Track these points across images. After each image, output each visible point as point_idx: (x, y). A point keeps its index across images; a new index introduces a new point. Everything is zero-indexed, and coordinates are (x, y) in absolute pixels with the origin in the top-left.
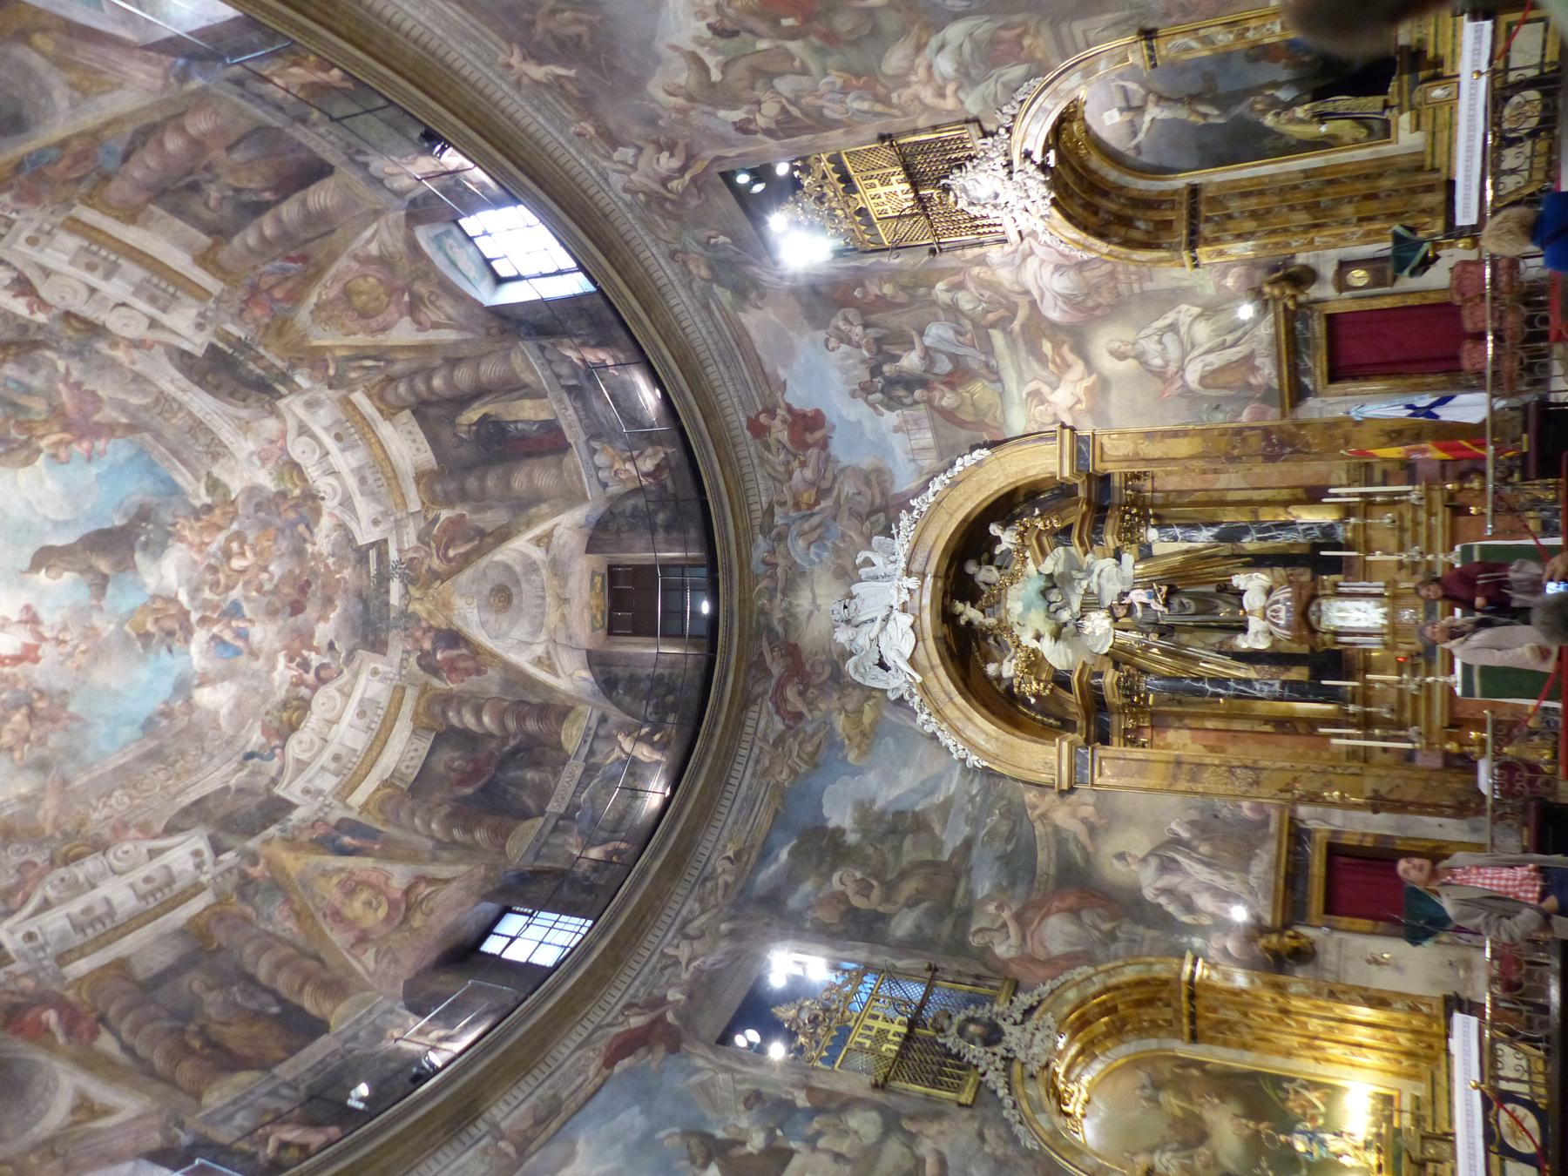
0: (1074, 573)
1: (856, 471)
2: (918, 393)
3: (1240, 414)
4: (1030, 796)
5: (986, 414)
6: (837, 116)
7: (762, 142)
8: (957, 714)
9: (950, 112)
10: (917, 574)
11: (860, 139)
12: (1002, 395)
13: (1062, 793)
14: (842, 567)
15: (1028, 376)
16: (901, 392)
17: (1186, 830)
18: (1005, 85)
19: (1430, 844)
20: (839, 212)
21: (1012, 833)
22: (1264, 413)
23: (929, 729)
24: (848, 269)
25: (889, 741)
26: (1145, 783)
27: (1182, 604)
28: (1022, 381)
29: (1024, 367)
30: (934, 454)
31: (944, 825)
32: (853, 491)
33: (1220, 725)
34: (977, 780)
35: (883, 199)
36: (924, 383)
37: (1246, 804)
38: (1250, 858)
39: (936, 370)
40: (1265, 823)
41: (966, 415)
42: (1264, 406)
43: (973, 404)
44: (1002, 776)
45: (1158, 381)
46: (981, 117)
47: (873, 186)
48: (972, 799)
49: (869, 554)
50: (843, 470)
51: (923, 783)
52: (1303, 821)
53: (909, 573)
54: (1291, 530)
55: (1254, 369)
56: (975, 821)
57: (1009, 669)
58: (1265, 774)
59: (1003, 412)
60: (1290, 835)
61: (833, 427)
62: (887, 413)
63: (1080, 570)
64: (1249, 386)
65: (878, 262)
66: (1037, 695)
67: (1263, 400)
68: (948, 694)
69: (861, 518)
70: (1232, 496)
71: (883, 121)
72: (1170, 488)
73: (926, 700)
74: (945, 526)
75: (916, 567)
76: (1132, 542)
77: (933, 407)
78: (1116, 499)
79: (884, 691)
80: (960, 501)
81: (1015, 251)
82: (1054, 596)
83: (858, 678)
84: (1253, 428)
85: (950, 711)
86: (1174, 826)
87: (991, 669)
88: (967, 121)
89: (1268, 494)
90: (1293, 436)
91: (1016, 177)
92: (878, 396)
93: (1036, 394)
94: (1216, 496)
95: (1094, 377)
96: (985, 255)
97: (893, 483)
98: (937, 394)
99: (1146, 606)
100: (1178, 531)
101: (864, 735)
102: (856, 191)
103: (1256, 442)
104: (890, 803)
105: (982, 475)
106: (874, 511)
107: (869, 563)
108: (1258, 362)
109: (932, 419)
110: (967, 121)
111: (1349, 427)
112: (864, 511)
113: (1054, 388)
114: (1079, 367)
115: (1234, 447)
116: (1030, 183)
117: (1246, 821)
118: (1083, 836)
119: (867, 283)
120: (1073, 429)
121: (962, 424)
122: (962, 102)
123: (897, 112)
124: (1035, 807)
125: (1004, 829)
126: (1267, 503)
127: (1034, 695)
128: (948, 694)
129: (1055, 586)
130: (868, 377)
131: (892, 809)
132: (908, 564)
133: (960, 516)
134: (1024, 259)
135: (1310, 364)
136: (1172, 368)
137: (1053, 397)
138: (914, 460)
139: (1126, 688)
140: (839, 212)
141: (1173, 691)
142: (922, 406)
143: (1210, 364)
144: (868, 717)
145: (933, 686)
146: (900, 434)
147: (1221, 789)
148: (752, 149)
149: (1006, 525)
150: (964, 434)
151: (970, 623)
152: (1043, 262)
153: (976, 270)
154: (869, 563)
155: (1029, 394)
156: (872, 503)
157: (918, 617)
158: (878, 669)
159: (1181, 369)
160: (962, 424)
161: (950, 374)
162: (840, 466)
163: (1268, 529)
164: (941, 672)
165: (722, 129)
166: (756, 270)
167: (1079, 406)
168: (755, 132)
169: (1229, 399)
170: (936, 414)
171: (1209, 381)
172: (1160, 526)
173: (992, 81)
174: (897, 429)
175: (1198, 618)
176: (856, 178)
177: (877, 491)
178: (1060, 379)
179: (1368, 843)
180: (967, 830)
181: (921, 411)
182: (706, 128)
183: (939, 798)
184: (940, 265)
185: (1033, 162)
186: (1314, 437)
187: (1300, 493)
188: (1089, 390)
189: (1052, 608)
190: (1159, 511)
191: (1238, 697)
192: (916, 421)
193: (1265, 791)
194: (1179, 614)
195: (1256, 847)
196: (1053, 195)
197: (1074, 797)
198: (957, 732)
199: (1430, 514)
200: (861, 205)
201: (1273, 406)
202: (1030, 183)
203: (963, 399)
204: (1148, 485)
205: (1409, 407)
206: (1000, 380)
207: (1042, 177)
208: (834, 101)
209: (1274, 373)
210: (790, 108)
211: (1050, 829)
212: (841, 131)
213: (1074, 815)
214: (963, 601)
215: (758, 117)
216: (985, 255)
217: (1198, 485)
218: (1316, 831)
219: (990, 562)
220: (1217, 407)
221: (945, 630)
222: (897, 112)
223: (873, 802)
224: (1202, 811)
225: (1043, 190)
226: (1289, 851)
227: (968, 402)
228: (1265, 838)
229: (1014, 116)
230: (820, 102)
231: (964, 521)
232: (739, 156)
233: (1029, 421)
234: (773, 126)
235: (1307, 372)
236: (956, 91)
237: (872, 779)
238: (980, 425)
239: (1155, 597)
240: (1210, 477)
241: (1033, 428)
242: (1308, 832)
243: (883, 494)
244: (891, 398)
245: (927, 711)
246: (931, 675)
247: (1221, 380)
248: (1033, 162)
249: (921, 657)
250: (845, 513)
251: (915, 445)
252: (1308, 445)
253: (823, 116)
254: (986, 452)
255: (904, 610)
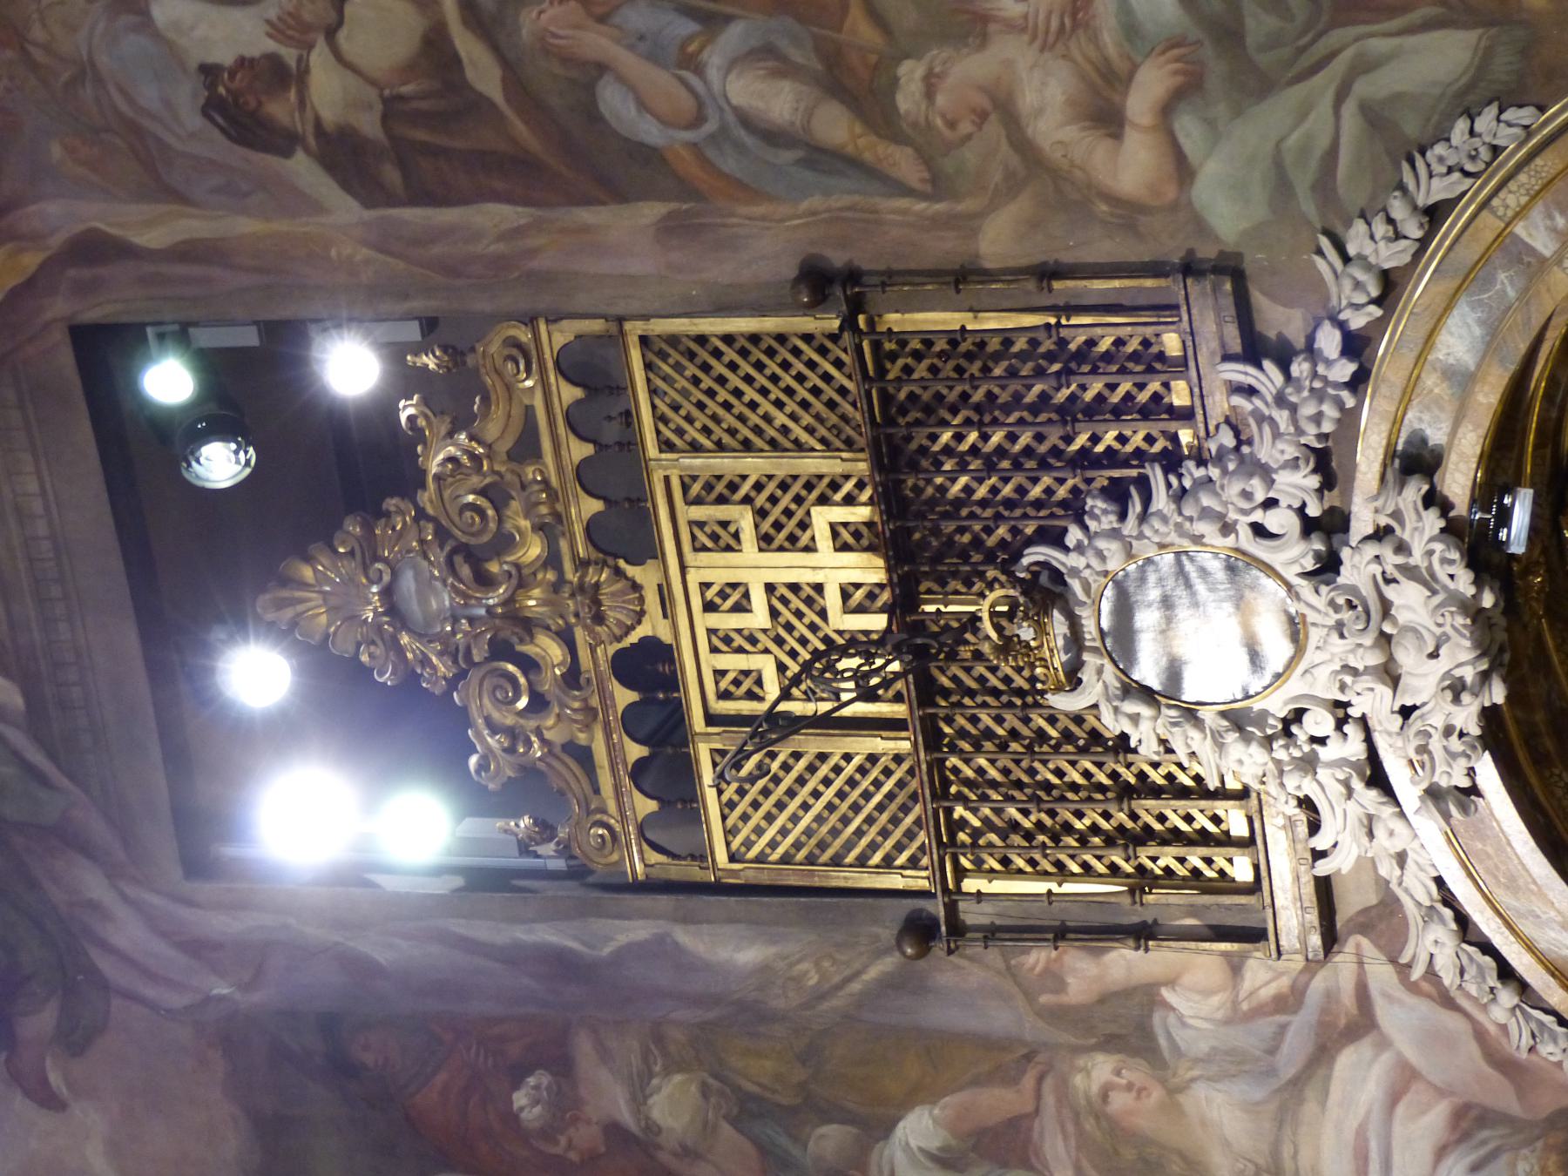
6: (650, 132)
7: (298, 202)
9: (1129, 213)
11: (722, 271)
18: (1376, 118)
20: (550, 650)
24: (514, 957)
35: (759, 618)
46: (1254, 260)
47: (724, 540)
65: (660, 949)
71: (841, 196)
81: (1288, 1002)
88: (1190, 268)
91: (1358, 568)
96: (1146, 997)
102: (648, 550)
110: (1190, 268)
116: (1409, 601)
119: (583, 1047)
122: (1183, 170)
123: (904, 163)
134: (1323, 1053)
140: (550, 650)
148: (245, 226)
152: (1404, 1080)
153: (1100, 1070)
165: (149, 95)
166: (93, 884)
168: (282, 142)
173: (1327, 82)
176: (664, 468)
182: (86, 71)
184: (941, 1016)
185: (1433, 499)
196: (1498, 694)
200: (653, 626)
202: (1409, 601)
207: (1464, 583)
208: (649, 47)
210: (467, 45)
212: (651, 211)
215: (319, 58)
216: (1146, 997)
222: (904, 163)
225: (1462, 657)
229: (1390, 286)
230: (596, 43)
232: (186, 252)
234: (369, 125)
236: (1167, 111)
248: (1433, 499)
253: (592, 115)
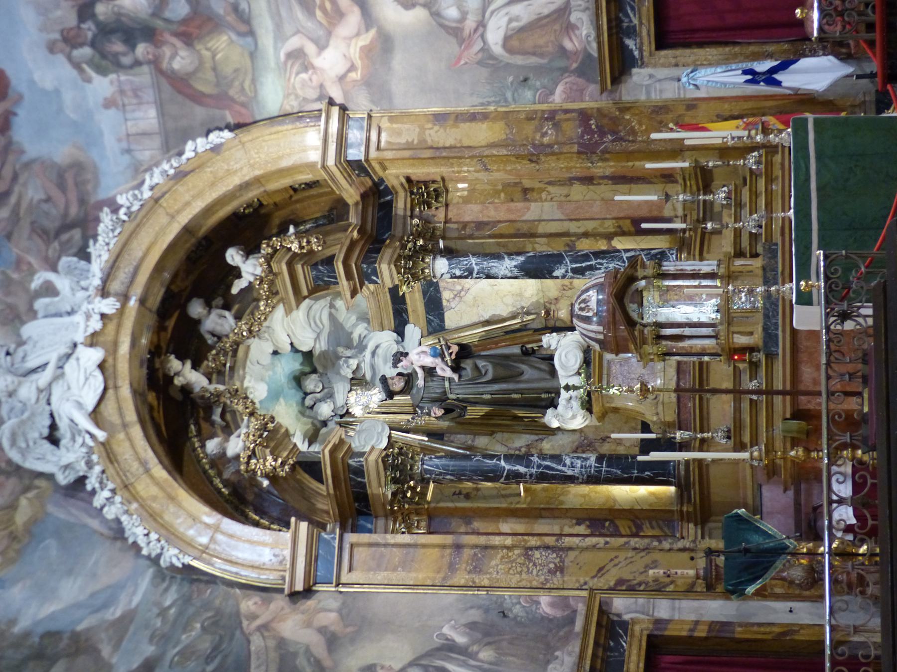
0: (340, 350)
1: (45, 165)
2: (142, 49)
3: (552, 93)
4: (249, 604)
5: (230, 85)
8: (154, 490)
10: (116, 295)
12: (253, 55)
13: (294, 596)
14: (11, 307)
15: (288, 28)
16: (118, 47)
17: (463, 634)
19: (777, 630)
21: (216, 649)
22: (582, 91)
23: (110, 513)
25: (52, 546)
26: (411, 577)
27: (476, 368)
28: (280, 36)
29: (284, 13)
30: (157, 142)
31: (117, 646)
32: (41, 195)
33: (520, 527)
34: (174, 588)
36: (149, 33)
37: (545, 600)
38: (548, 662)
39: (167, 14)
40: (571, 620)
41: (202, 86)
42: (581, 81)
43: (214, 69)
44: (212, 580)
45: (453, 40)
48: (163, 612)
49: (51, 276)
50: (28, 165)
51: (93, 595)
52: (619, 615)
53: (104, 293)
54: (613, 258)
55: (570, 28)
56: (163, 639)
57: (235, 446)
58: (572, 555)
59: (254, 81)
60: (599, 624)
61: (20, 98)
62: (97, 78)
63: (349, 346)
64: (563, 51)
66: (273, 477)
67: (581, 72)
68: (144, 464)
69: (46, 235)
70: (542, 229)
72: (467, 218)
73: (111, 471)
74: (163, 230)
75: (116, 286)
76: (415, 278)
77: (160, 71)
78: (398, 230)
79: (50, 477)
80: (187, 197)
82: (312, 383)
83: (14, 456)
84: (566, 111)
85: (145, 488)
86: (446, 630)
87: (212, 446)
89: (590, 226)
90: (615, 121)
92: (87, 51)
93: (297, 55)
94: (525, 228)
95: (373, 32)
97: (97, 185)
98: (167, 51)
99: (430, 372)
100: (473, 260)
101: (13, 537)
103: (572, 129)
104: (38, 623)
105: (219, 165)
106: (66, 227)
107: (49, 290)
108: (574, 18)
109: (158, 89)
111: (681, 110)
112: (52, 225)
113: (322, 47)
114: (354, 18)
115: (544, 134)
117: (545, 620)
118: (320, 649)
120: (343, 109)
121: (198, 98)
124: (253, 617)
125: (206, 645)
126: (586, 235)
127: (267, 476)
128: (144, 464)
129: (314, 371)
130: (72, 20)
131: (41, 630)
132: (105, 281)
133: (184, 219)
135: (636, 21)
136: (470, 23)
137: (318, 62)
138: (128, 151)
139: (394, 468)
141: (460, 476)
142: (145, 68)
143: (517, 19)
144: (22, 516)
145: (123, 450)
146: (112, 112)
147: (514, 580)
149: (250, 250)
150: (200, 113)
151: (186, 390)
154: (49, 290)
155: (290, 55)
156: (66, 214)
157: (112, 349)
158: (47, 445)
159: (482, 25)
160: (198, 98)
161: (185, 21)
162: (25, 158)
163: (586, 257)
164: (137, 432)
167: (353, 75)
169: (539, 70)
170: (164, 83)
171: (515, 43)
172: (450, 253)
174: (109, 104)
175: (496, 387)
177: (73, 196)
178: (329, 34)
179: (701, 632)
180: (149, 650)
181: (144, 77)
183: (115, 612)
186: (641, 125)
187: (627, 225)
188: (367, 51)
189: (309, 401)
190: (452, 244)
191: (542, 478)
192: (136, 92)
193: (570, 580)
194: (472, 381)
195: (557, 649)
197: (311, 603)
198: (152, 517)
199: (770, 180)
201: (590, 80)
203: (201, 62)
204: (441, 215)
205: (745, 72)
206: (251, 33)
209: (593, 35)
211: (271, 643)
213: (308, 624)
214: (181, 358)
217: (502, 215)
218: (634, 621)
219: (227, 307)
220: (526, 80)
221: (151, 397)
223: (13, 622)
224: (487, 611)
226: (596, 644)
227: (208, 65)
228: (566, 639)
231: (187, 230)
233: (287, 96)
235: (632, 32)
237: (16, 593)
238: (222, 99)
239: (442, 356)
240: (520, 205)
241: (292, 105)
242: (624, 625)
243: (82, 201)
244: (104, 56)
245: (110, 486)
246: (122, 436)
247: (529, 44)
249: (109, 410)
250: (25, 225)
251: (133, 130)
252: (633, 132)
254: (227, 134)
255: (93, 340)
